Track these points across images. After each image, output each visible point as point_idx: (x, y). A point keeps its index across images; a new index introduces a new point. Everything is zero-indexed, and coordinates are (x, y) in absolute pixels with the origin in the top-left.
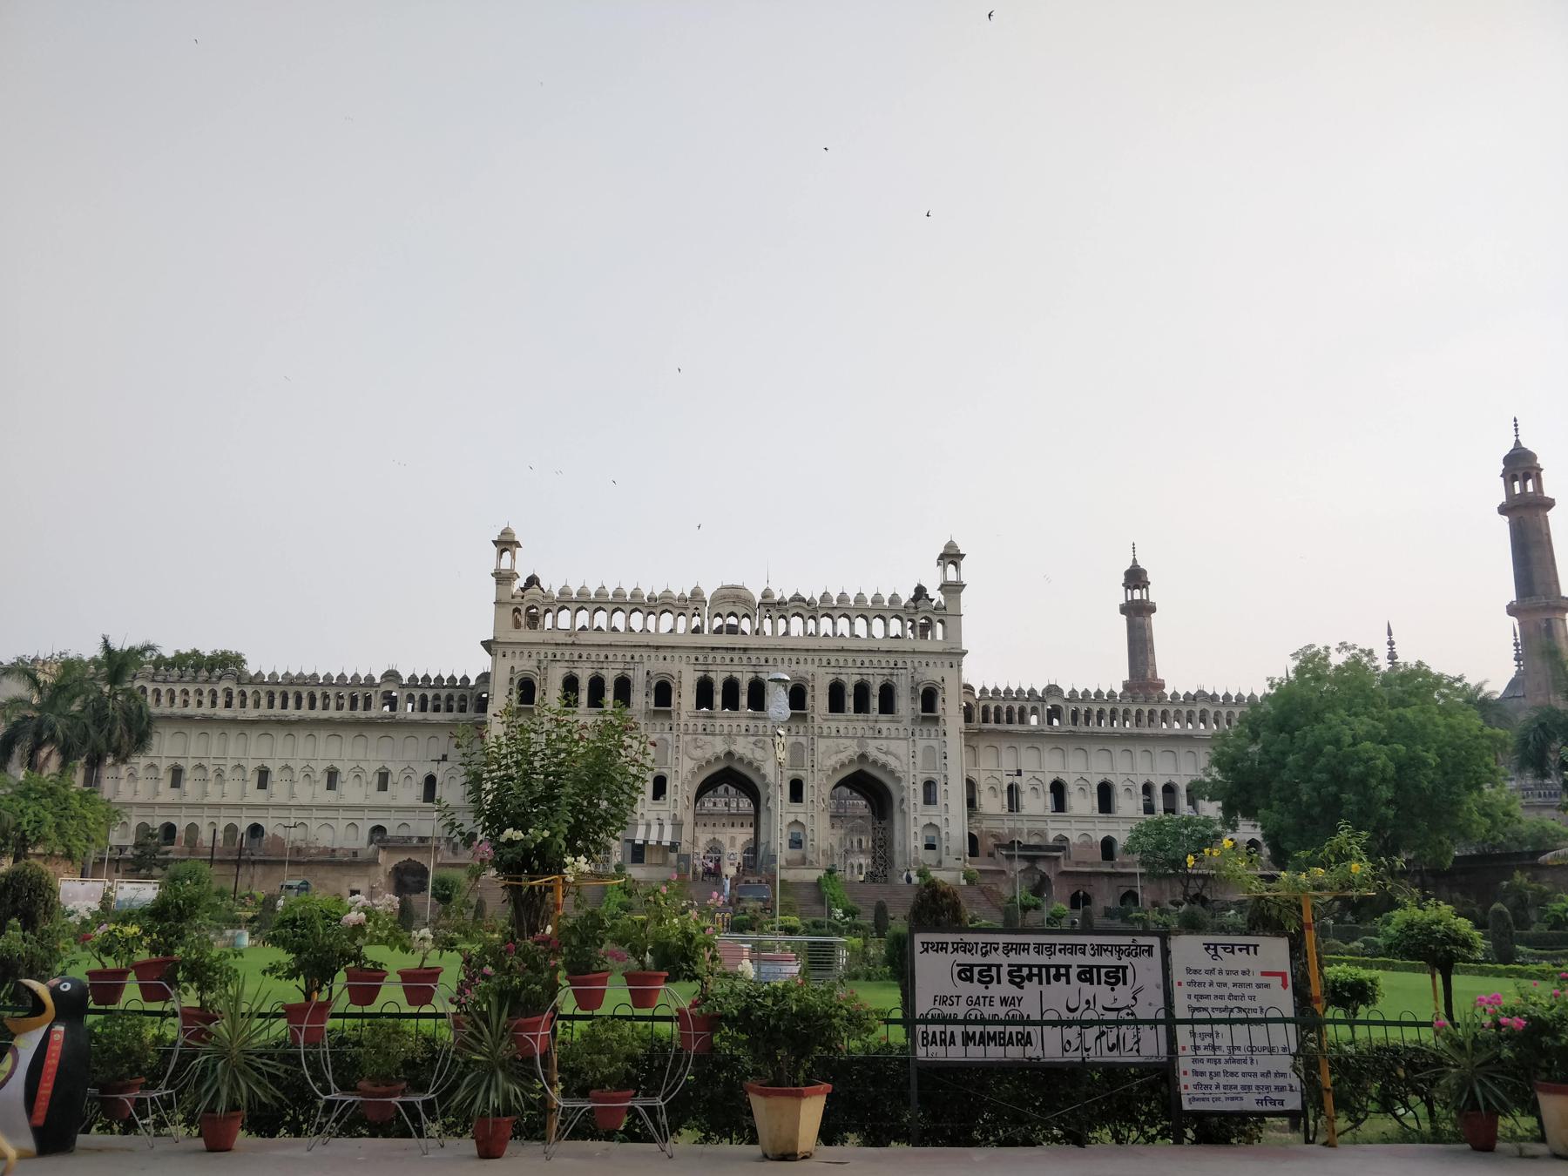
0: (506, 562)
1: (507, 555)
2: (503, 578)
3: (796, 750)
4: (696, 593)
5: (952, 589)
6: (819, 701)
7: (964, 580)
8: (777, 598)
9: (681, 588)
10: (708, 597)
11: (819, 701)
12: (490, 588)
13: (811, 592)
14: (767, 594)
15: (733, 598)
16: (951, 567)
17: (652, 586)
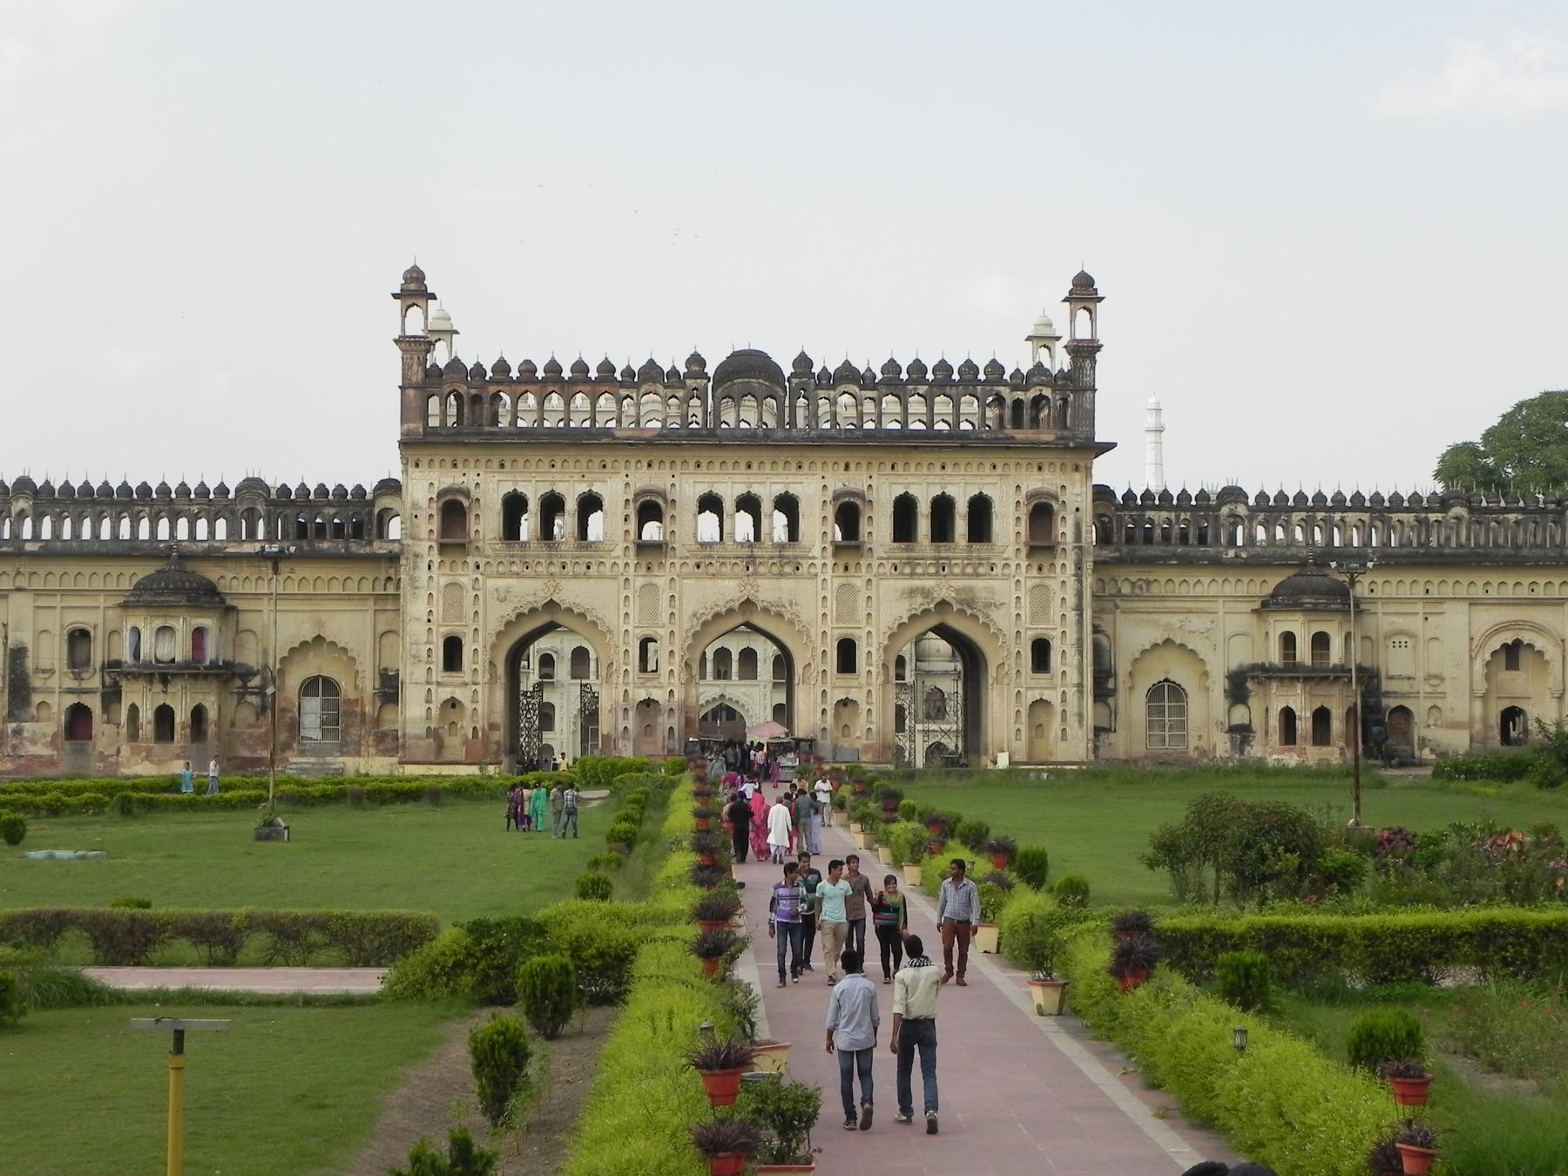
0: (415, 327)
2: (415, 347)
4: (696, 361)
5: (1085, 352)
6: (878, 527)
7: (1102, 338)
8: (816, 369)
9: (672, 358)
10: (710, 370)
11: (878, 527)
12: (391, 367)
13: (870, 360)
14: (803, 362)
15: (749, 370)
16: (1083, 315)
17: (628, 358)
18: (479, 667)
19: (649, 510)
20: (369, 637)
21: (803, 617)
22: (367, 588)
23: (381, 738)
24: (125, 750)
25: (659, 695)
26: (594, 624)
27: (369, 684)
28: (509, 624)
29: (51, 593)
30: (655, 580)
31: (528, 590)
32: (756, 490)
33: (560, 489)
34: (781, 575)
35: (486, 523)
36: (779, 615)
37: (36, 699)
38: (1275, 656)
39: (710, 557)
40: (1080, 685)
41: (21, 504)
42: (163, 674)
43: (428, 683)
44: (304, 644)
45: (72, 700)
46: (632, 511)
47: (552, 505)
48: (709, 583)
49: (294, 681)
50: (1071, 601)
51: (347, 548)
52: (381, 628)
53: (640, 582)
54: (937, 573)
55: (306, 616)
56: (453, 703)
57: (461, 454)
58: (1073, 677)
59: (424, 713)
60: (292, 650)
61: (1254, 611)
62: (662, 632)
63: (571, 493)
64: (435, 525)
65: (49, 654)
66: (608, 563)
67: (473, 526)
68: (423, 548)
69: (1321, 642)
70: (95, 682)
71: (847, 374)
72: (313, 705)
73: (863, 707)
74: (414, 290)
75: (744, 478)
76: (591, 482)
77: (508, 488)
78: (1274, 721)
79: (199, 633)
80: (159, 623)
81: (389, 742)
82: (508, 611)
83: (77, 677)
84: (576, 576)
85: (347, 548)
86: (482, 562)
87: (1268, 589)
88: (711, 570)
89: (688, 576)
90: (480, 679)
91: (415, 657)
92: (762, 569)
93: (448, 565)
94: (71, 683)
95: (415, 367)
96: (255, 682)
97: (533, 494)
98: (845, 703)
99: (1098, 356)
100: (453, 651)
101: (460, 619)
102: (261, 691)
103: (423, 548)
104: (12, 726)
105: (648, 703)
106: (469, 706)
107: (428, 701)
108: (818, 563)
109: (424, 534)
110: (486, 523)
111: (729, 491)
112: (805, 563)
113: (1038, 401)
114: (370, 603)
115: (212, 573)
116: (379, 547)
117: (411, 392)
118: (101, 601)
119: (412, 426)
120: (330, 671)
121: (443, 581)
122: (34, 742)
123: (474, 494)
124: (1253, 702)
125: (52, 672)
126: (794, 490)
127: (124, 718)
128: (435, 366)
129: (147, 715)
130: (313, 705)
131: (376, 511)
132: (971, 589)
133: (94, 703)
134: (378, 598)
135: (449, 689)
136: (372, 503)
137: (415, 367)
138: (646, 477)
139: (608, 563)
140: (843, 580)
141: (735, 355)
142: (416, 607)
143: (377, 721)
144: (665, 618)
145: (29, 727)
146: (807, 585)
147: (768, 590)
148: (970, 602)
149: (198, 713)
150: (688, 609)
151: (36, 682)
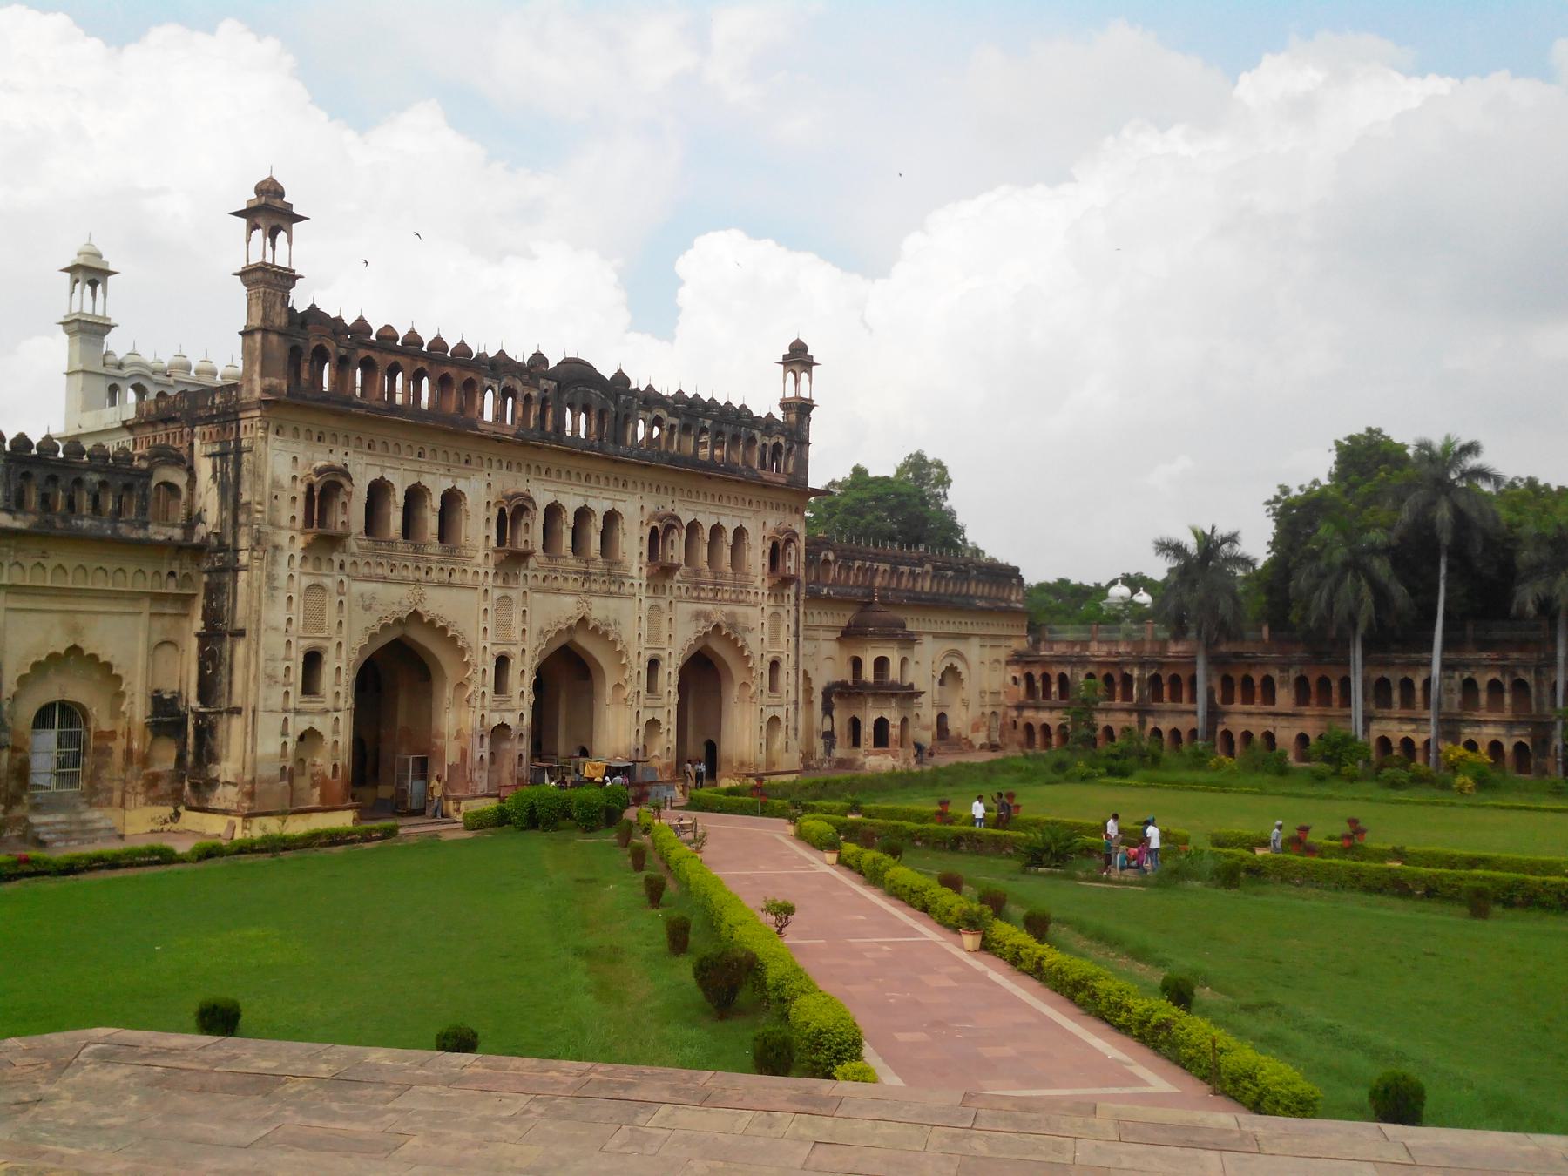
2: (268, 282)
9: (520, 353)
13: (666, 388)
15: (577, 379)
17: (484, 344)
18: (342, 690)
19: (510, 515)
20: (141, 647)
21: (624, 637)
22: (143, 586)
23: (153, 781)
25: (511, 719)
26: (454, 639)
27: (138, 709)
30: (511, 593)
31: (393, 599)
33: (427, 481)
34: (610, 594)
38: (868, 674)
39: (555, 570)
40: (796, 703)
43: (285, 710)
44: (54, 657)
48: (554, 598)
49: (28, 710)
50: (792, 628)
51: (115, 529)
52: (156, 639)
53: (497, 593)
54: (714, 599)
55: (56, 618)
57: (332, 423)
58: (792, 696)
59: (278, 749)
60: (37, 666)
61: (838, 639)
62: (515, 651)
66: (470, 570)
69: (881, 664)
71: (651, 399)
72: (48, 740)
73: (664, 727)
74: (270, 211)
75: (582, 491)
76: (455, 478)
78: (867, 730)
82: (371, 621)
84: (440, 584)
85: (115, 529)
86: (348, 561)
87: (844, 623)
88: (556, 584)
89: (534, 590)
90: (341, 704)
91: (270, 677)
92: (595, 587)
93: (311, 560)
95: (278, 307)
97: (400, 483)
99: (812, 414)
101: (320, 629)
103: (283, 538)
105: (502, 730)
106: (328, 737)
107: (284, 733)
108: (636, 583)
109: (285, 521)
111: (571, 503)
112: (628, 582)
113: (777, 446)
114: (145, 607)
116: (157, 532)
117: (274, 338)
119: (275, 381)
120: (76, 690)
121: (306, 581)
124: (835, 713)
126: (620, 507)
128: (292, 310)
130: (48, 740)
131: (154, 483)
132: (732, 615)
134: (158, 598)
135: (307, 718)
136: (147, 474)
137: (278, 307)
139: (470, 570)
140: (652, 602)
143: (146, 760)
144: (517, 635)
146: (627, 604)
147: (600, 609)
148: (733, 626)
150: (536, 624)
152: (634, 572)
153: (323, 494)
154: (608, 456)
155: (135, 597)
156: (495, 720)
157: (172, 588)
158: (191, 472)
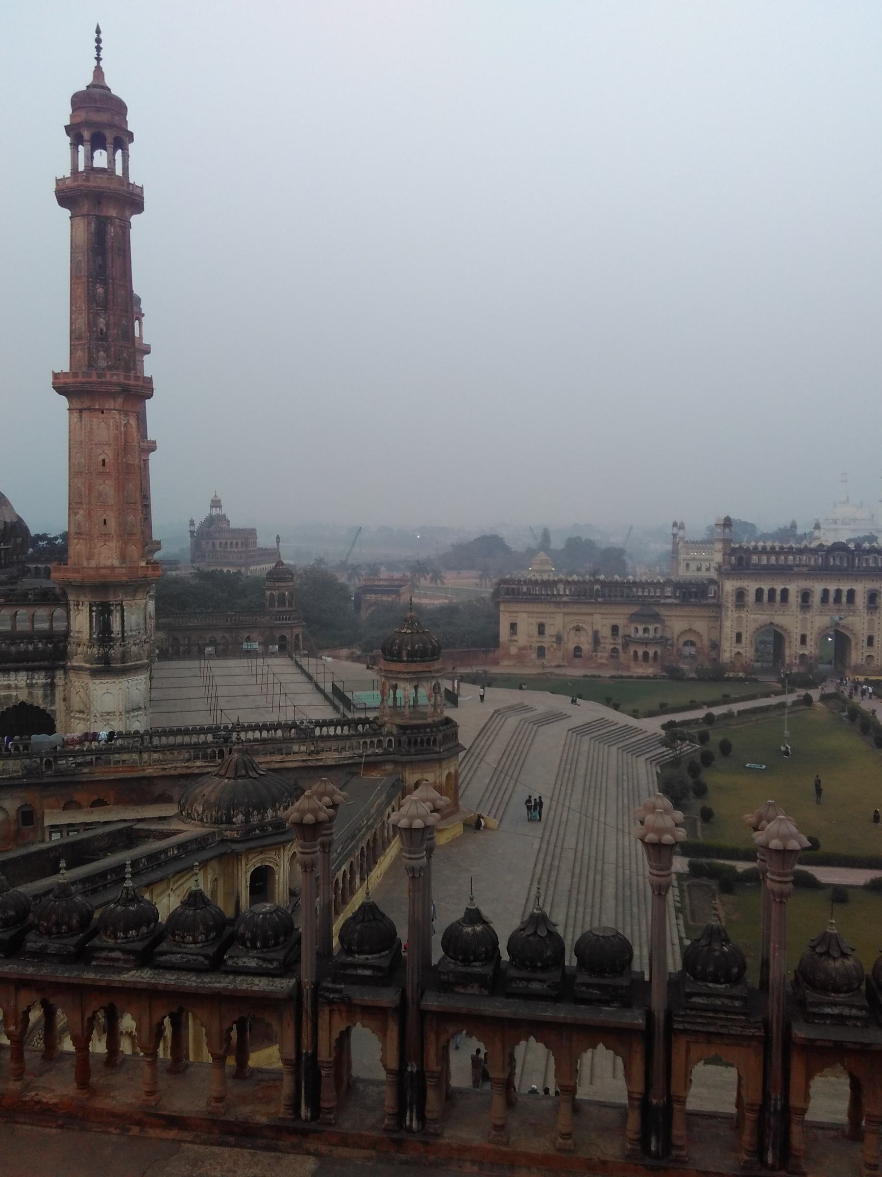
1: (727, 530)
3: (871, 622)
24: (632, 664)
25: (806, 653)
27: (706, 643)
28: (757, 629)
29: (607, 614)
32: (841, 588)
33: (775, 587)
35: (751, 597)
36: (848, 628)
37: (602, 646)
41: (597, 587)
42: (645, 642)
45: (613, 646)
46: (799, 595)
47: (772, 592)
49: (682, 640)
53: (800, 617)
56: (738, 653)
60: (682, 633)
63: (779, 587)
64: (734, 598)
65: (606, 632)
67: (746, 599)
68: (730, 605)
70: (620, 641)
77: (758, 587)
79: (656, 630)
80: (644, 626)
81: (715, 661)
82: (757, 625)
83: (615, 639)
94: (612, 641)
96: (670, 642)
97: (766, 587)
98: (869, 656)
100: (739, 636)
102: (672, 645)
103: (730, 605)
104: (594, 654)
105: (803, 655)
106: (744, 654)
110: (751, 597)
111: (832, 587)
115: (657, 609)
116: (710, 601)
118: (622, 616)
121: (736, 615)
122: (601, 658)
123: (747, 588)
125: (606, 638)
126: (854, 588)
127: (632, 653)
129: (640, 653)
133: (620, 647)
138: (804, 584)
141: (835, 543)
142: (727, 624)
145: (599, 654)
149: (656, 653)
151: (602, 641)
152: (861, 608)
153: (740, 594)
154: (851, 572)
155: (703, 617)
156: (801, 652)
157: (714, 614)
158: (719, 586)
